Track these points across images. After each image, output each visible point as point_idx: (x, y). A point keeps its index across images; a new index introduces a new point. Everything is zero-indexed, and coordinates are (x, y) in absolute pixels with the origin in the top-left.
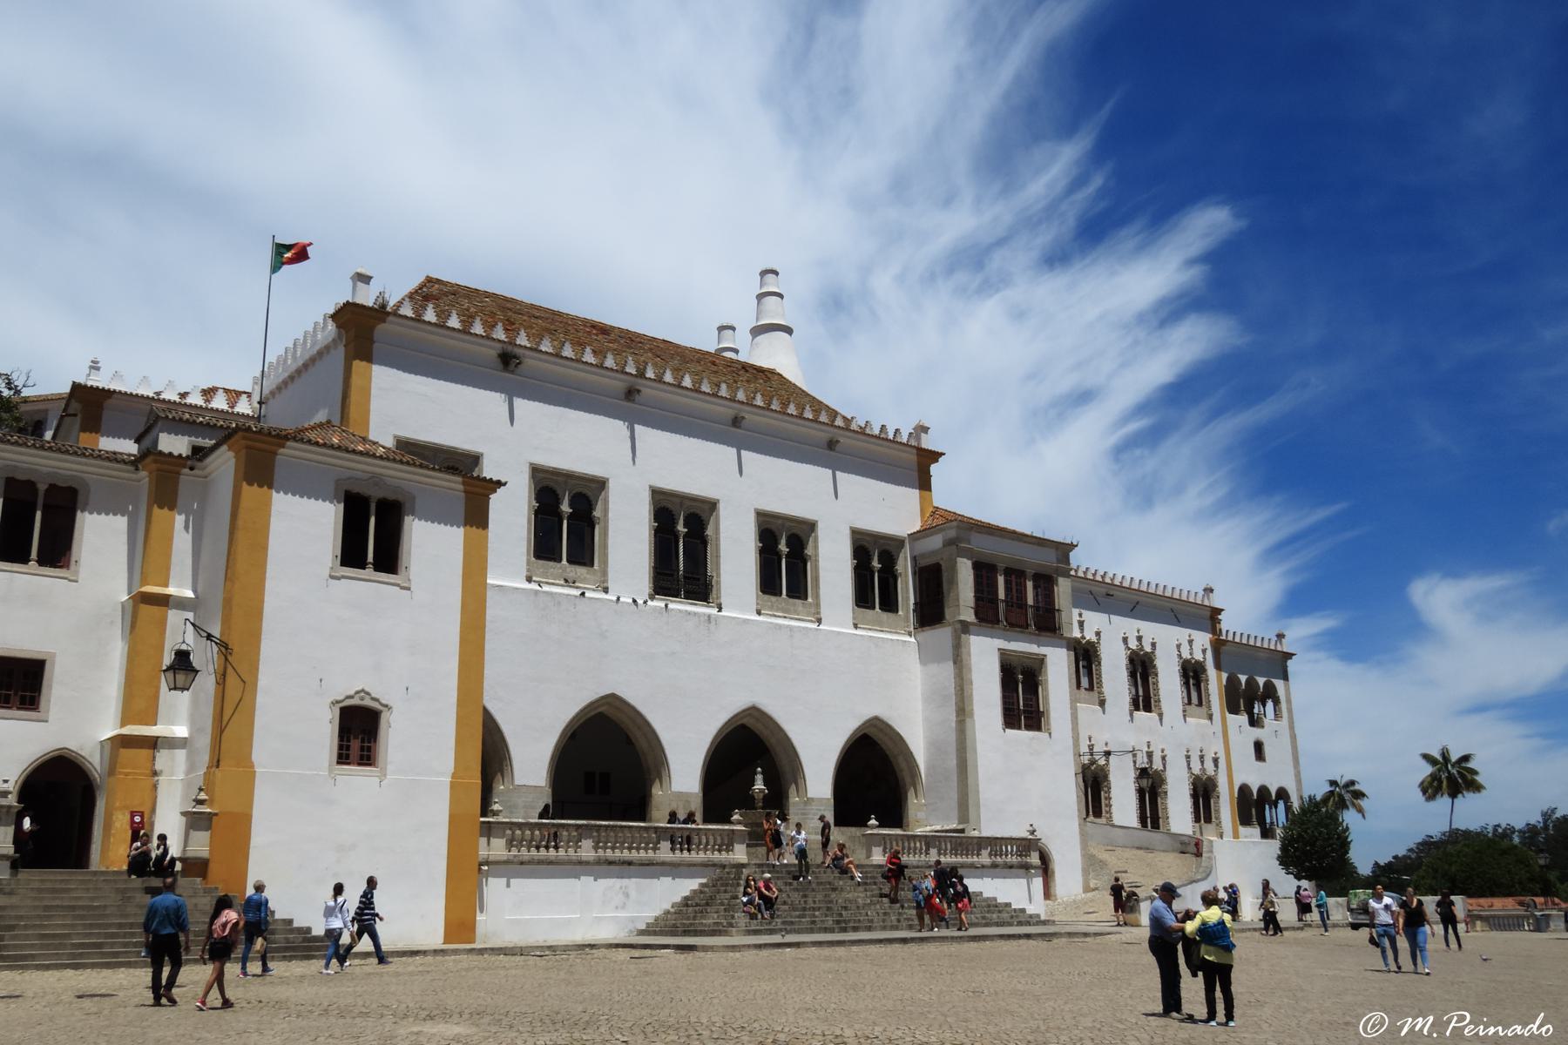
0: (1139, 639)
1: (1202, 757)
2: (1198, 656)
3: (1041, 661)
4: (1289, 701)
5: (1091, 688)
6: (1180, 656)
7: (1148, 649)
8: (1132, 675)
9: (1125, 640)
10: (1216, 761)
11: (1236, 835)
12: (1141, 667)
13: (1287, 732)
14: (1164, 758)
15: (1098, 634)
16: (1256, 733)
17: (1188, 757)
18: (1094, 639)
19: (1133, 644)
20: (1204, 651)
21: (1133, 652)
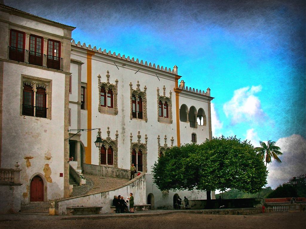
0: (138, 85)
1: (166, 139)
2: (168, 95)
3: (50, 82)
4: (210, 118)
5: (112, 107)
7: (142, 90)
8: (134, 102)
9: (131, 85)
10: (172, 140)
12: (138, 98)
13: (208, 130)
14: (146, 139)
15: (117, 82)
16: (193, 130)
17: (159, 139)
18: (114, 84)
19: (135, 88)
20: (171, 93)
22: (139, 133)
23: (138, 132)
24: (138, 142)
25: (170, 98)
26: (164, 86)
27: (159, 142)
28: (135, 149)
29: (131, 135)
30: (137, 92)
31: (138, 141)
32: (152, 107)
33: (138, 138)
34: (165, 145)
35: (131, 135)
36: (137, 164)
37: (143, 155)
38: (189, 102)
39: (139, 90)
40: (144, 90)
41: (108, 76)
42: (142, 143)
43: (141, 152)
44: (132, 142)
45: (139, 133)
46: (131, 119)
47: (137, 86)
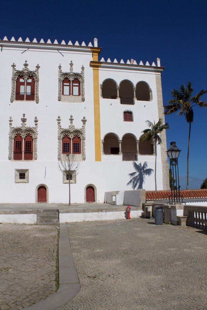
0: (26, 65)
6: (61, 71)
9: (14, 66)
10: (84, 121)
11: (98, 159)
14: (36, 121)
17: (59, 120)
20: (83, 68)
21: (18, 72)
22: (24, 116)
23: (22, 115)
24: (21, 126)
25: (82, 73)
26: (71, 62)
27: (59, 123)
28: (21, 134)
29: (11, 119)
30: (24, 72)
31: (22, 124)
32: (48, 85)
33: (22, 121)
34: (69, 126)
35: (11, 119)
36: (23, 151)
37: (34, 140)
38: (118, 76)
40: (36, 68)
42: (28, 127)
43: (31, 137)
44: (12, 126)
45: (24, 116)
46: (12, 102)
47: (24, 66)
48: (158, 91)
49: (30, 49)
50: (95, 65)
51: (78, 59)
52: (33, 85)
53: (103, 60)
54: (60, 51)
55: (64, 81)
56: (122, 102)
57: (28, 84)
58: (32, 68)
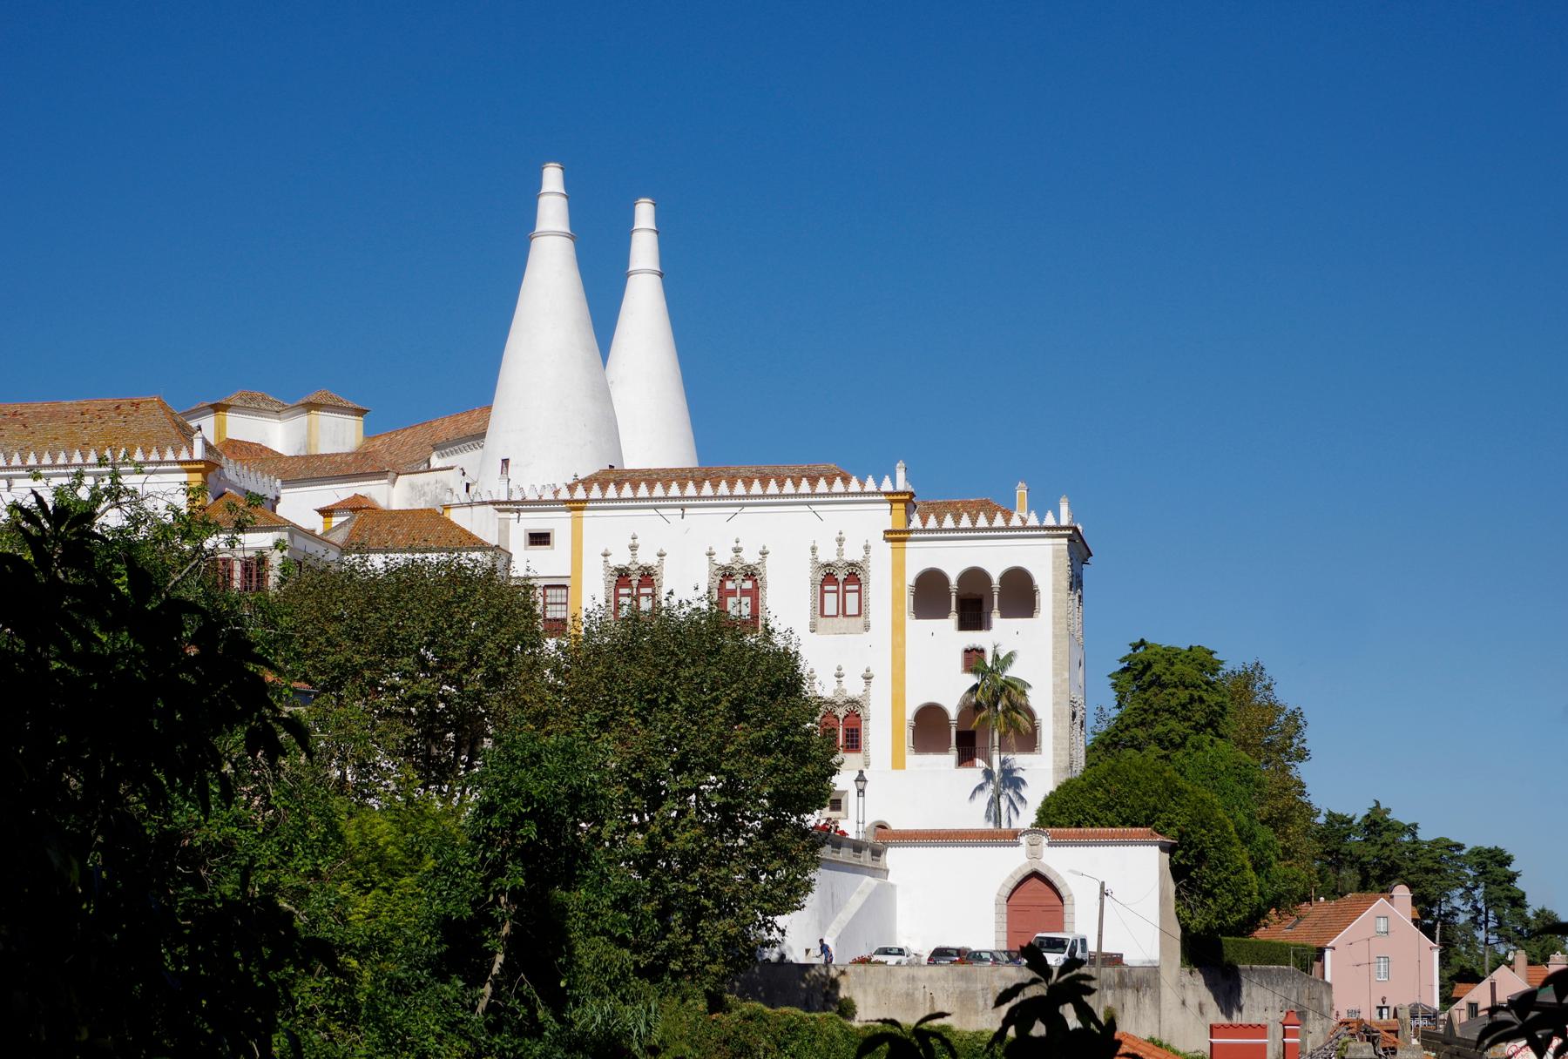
0: (737, 550)
10: (868, 678)
11: (898, 763)
19: (724, 558)
20: (867, 548)
38: (953, 559)
39: (738, 560)
41: (633, 548)
48: (1055, 590)
49: (746, 509)
50: (896, 537)
51: (856, 525)
52: (754, 594)
53: (916, 522)
54: (814, 508)
55: (824, 582)
56: (964, 625)
57: (745, 593)
58: (750, 557)
